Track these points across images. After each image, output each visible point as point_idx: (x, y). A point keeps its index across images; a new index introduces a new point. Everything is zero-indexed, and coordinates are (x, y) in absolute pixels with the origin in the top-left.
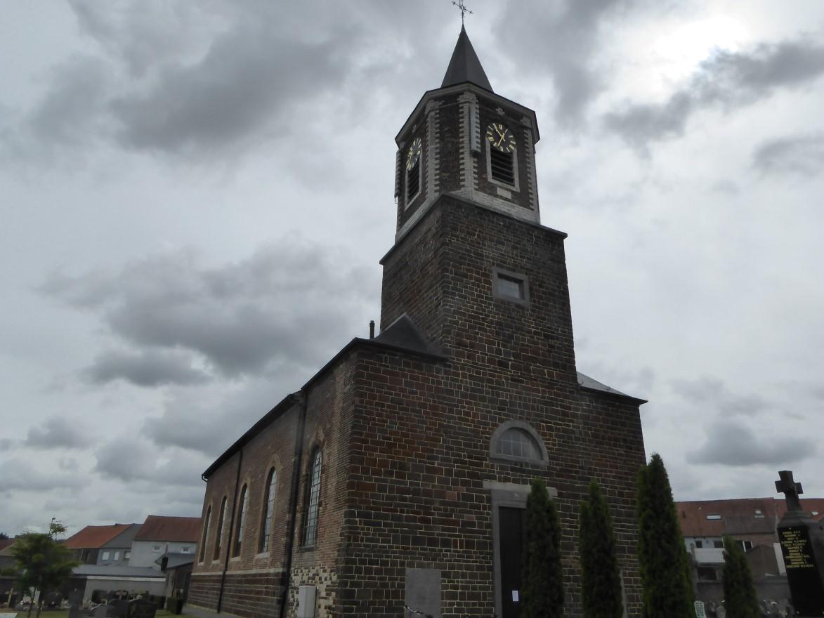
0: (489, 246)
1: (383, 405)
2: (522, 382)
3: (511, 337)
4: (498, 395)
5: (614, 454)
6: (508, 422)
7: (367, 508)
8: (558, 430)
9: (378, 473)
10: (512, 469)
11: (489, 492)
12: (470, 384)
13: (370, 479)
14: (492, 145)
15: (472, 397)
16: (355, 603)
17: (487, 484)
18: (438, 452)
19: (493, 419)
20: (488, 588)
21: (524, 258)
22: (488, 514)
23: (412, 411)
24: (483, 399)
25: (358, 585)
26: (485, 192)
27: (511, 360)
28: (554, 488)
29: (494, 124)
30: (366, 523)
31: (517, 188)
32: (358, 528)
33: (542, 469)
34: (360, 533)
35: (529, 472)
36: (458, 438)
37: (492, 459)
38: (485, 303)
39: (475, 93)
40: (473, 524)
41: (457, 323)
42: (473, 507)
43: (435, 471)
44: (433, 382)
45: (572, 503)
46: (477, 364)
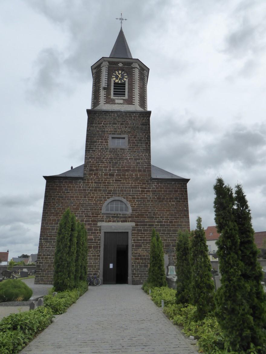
0: (109, 127)
1: (55, 199)
2: (121, 181)
3: (116, 163)
4: (108, 188)
5: (169, 205)
6: (112, 198)
7: (47, 236)
8: (137, 198)
9: (52, 223)
10: (112, 217)
11: (100, 227)
12: (95, 185)
13: (49, 226)
14: (114, 82)
15: (95, 190)
16: (40, 269)
17: (99, 224)
19: (105, 198)
20: (97, 263)
21: (127, 127)
22: (99, 235)
23: (67, 199)
25: (42, 263)
26: (110, 104)
27: (116, 173)
28: (134, 223)
29: (116, 72)
30: (46, 242)
31: (126, 97)
32: (43, 244)
33: (128, 215)
34: (43, 245)
35: (121, 217)
36: (87, 207)
37: (103, 214)
38: (104, 151)
39: (107, 61)
40: (92, 239)
45: (142, 228)
46: (99, 177)
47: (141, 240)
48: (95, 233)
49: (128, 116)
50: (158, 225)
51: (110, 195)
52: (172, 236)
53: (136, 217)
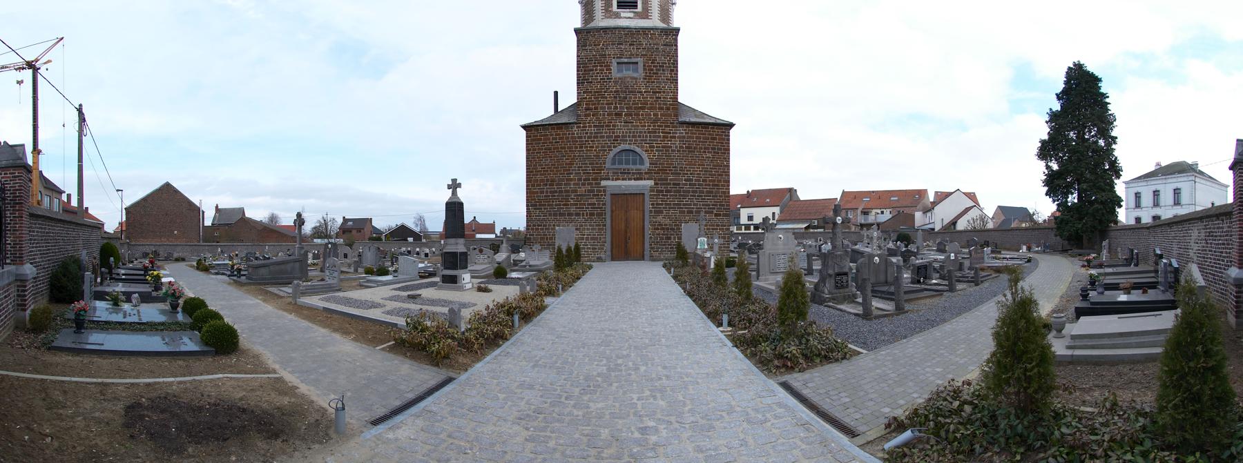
2: (633, 123)
4: (613, 133)
10: (621, 173)
11: (605, 187)
12: (594, 130)
15: (597, 137)
17: (604, 183)
18: (573, 170)
19: (608, 147)
20: (603, 235)
24: (603, 137)
38: (606, 82)
41: (586, 98)
42: (595, 195)
43: (571, 180)
44: (569, 134)
47: (662, 204)
48: (598, 195)
49: (641, 34)
50: (686, 185)
51: (617, 143)
52: (705, 199)
53: (655, 173)
